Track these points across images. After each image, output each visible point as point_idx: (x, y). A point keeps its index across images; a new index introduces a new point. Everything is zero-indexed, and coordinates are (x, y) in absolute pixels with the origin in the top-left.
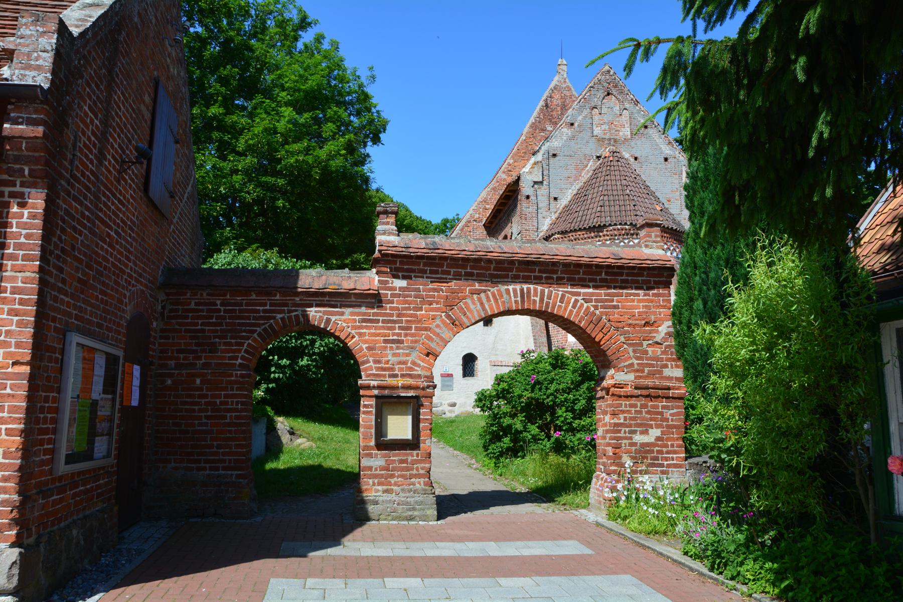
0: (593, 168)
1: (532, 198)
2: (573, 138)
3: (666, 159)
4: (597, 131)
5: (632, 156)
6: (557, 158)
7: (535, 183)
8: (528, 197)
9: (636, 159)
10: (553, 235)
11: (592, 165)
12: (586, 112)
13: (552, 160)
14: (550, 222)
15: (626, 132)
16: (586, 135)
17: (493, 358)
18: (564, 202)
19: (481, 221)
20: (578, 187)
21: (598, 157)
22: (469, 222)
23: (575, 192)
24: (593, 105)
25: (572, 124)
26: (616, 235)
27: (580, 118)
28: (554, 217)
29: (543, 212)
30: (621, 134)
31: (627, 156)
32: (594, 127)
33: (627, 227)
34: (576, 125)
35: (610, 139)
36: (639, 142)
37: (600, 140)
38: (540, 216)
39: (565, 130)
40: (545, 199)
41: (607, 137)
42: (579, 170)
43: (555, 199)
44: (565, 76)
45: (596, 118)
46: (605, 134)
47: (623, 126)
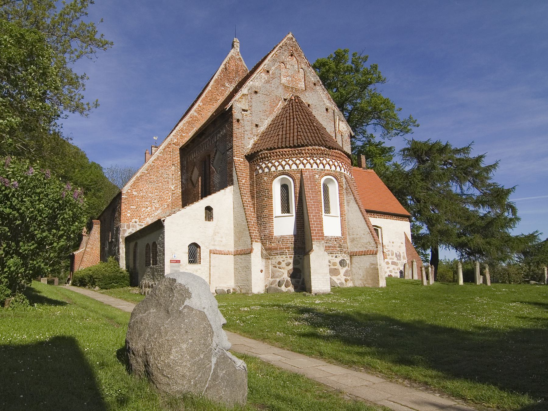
0: (282, 107)
1: (241, 121)
2: (268, 82)
3: (327, 110)
4: (284, 80)
5: (306, 103)
6: (258, 95)
7: (244, 110)
8: (238, 121)
9: (309, 105)
10: (261, 150)
11: (281, 105)
12: (277, 64)
13: (254, 96)
14: (253, 143)
15: (302, 85)
16: (276, 81)
17: (212, 248)
18: (262, 128)
19: (179, 145)
20: (271, 119)
21: (285, 100)
22: (170, 144)
23: (270, 122)
24: (282, 60)
25: (268, 72)
26: (315, 154)
27: (273, 68)
28: (256, 138)
29: (247, 135)
30: (299, 85)
31: (304, 102)
32: (282, 77)
33: (322, 148)
34: (271, 72)
35: (292, 88)
36: (311, 94)
37: (286, 87)
38: (246, 137)
39: (263, 74)
40: (249, 124)
41: (290, 86)
42: (273, 107)
43: (257, 126)
44: (238, 50)
45: (283, 71)
46: (289, 84)
47: (300, 80)
